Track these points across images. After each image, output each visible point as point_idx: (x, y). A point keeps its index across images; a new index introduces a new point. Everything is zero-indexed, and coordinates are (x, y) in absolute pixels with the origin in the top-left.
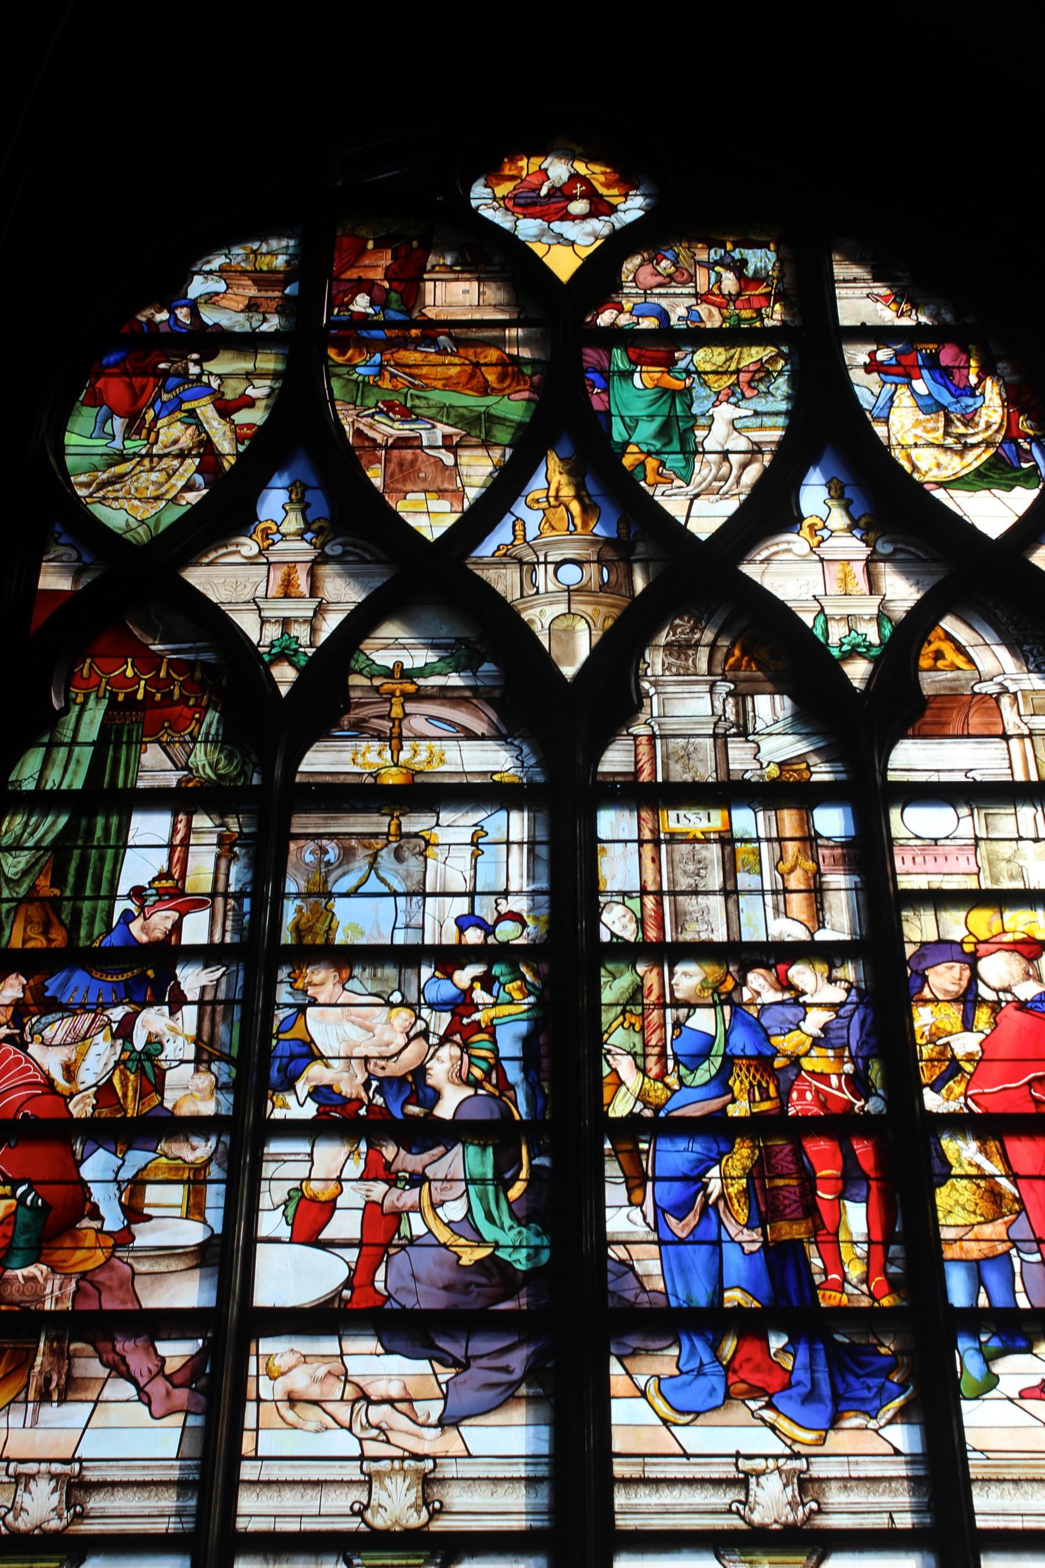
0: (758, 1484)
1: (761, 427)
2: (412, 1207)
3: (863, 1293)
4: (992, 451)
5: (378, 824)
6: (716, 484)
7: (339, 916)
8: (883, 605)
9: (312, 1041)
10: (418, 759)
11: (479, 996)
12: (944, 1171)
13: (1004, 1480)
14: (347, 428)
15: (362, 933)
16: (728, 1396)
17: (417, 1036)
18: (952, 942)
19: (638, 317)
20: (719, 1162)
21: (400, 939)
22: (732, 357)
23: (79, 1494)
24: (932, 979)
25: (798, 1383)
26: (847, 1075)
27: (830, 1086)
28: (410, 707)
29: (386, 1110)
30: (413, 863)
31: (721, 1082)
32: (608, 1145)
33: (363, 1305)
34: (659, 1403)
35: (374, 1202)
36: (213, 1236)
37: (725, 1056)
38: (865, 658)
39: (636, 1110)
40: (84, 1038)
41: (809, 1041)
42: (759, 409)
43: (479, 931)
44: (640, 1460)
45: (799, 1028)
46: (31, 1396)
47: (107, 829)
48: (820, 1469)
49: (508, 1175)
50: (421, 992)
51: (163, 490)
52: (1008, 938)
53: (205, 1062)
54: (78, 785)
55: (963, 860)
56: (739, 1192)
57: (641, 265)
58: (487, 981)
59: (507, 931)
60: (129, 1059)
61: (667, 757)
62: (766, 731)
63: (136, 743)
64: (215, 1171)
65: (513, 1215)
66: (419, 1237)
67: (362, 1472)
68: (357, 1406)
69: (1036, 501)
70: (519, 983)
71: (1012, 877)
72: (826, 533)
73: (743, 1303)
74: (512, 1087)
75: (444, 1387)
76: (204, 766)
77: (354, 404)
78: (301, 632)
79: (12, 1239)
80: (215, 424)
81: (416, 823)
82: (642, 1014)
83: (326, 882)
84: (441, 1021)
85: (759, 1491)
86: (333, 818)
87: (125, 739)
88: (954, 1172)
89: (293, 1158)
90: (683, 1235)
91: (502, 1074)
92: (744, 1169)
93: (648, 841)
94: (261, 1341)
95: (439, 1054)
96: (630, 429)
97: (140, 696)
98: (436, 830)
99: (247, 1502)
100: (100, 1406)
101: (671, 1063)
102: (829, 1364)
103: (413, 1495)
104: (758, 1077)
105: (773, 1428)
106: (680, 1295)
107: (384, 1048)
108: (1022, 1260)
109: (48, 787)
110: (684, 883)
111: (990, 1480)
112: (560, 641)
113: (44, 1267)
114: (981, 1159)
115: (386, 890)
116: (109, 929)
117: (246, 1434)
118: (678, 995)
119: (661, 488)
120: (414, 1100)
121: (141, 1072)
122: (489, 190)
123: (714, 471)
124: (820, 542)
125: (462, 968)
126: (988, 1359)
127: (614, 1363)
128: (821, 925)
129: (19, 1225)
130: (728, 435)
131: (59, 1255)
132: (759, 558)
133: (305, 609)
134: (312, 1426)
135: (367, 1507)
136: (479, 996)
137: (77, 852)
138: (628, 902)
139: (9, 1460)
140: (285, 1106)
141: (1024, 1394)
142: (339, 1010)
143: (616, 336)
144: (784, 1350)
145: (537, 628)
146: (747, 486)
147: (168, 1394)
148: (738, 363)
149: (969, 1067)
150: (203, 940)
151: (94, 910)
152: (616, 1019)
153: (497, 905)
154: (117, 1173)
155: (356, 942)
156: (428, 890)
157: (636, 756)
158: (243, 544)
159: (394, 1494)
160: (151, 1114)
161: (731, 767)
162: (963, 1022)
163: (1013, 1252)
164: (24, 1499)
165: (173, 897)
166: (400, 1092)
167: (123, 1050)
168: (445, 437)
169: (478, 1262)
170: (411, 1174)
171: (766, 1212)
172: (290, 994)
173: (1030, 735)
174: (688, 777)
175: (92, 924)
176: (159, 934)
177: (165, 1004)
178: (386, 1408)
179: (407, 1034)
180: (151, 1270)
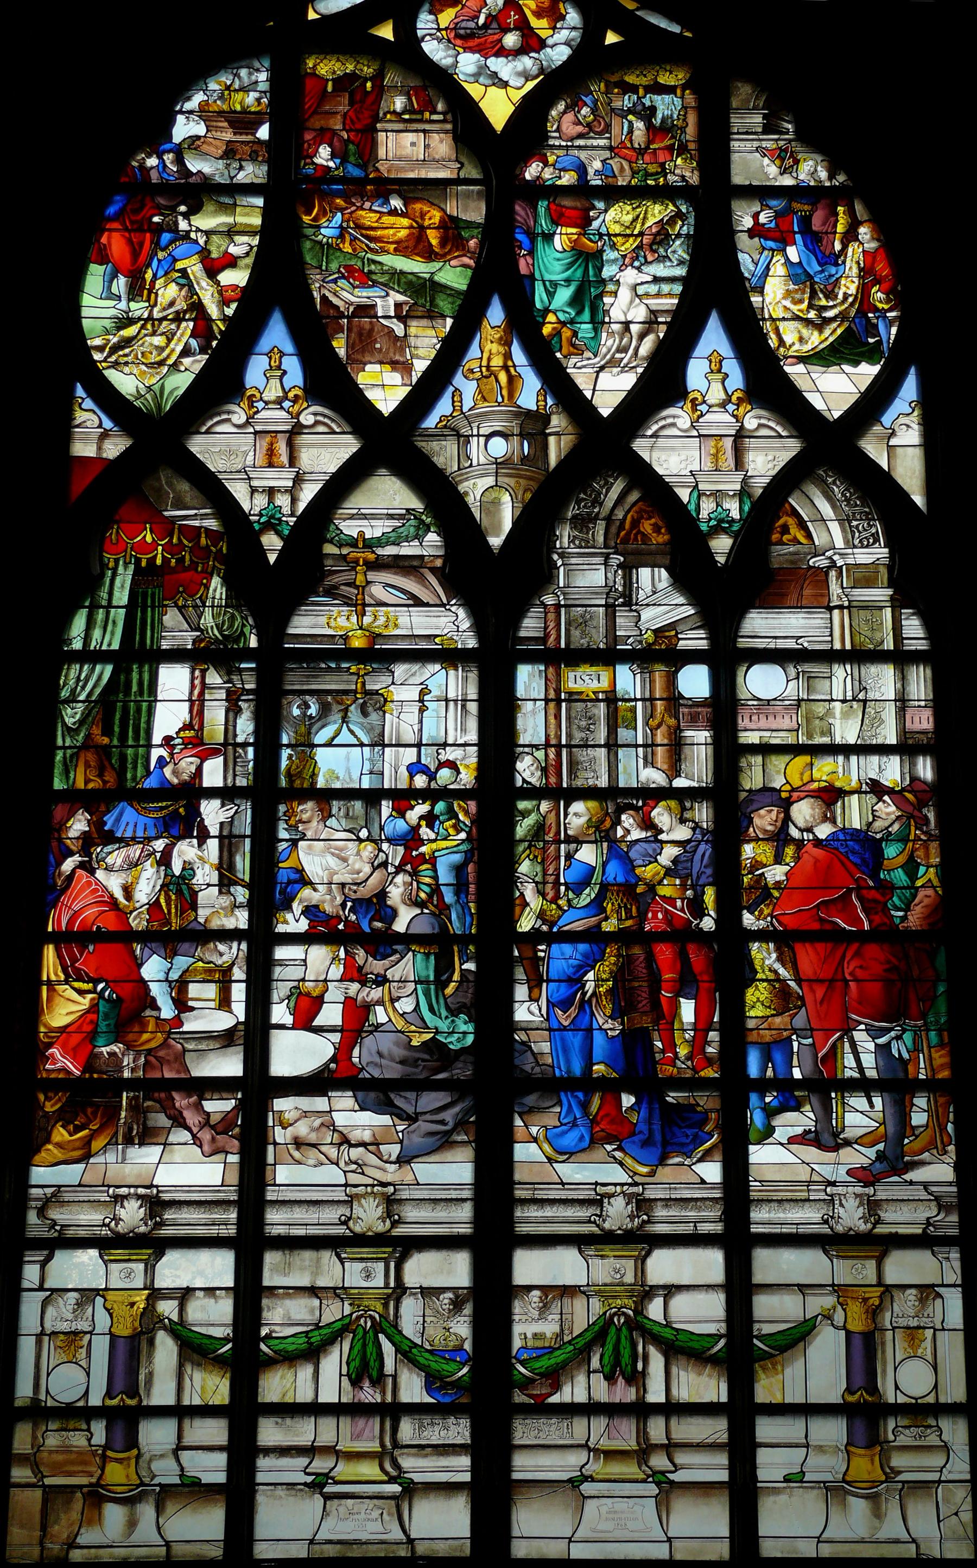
1: (658, 295)
4: (846, 324)
5: (348, 682)
6: (618, 356)
7: (319, 764)
8: (745, 481)
9: (303, 869)
11: (425, 832)
12: (751, 976)
14: (315, 294)
15: (338, 778)
16: (592, 1141)
17: (379, 866)
18: (774, 789)
19: (560, 170)
21: (365, 785)
22: (638, 216)
24: (757, 821)
25: (640, 1132)
26: (689, 899)
27: (675, 908)
28: (371, 576)
30: (374, 717)
31: (597, 905)
32: (516, 953)
33: (344, 1075)
34: (546, 1147)
36: (238, 1023)
37: (601, 884)
38: (727, 533)
40: (136, 865)
41: (662, 873)
42: (658, 275)
45: (656, 861)
46: (120, 1141)
47: (140, 683)
48: (651, 1194)
50: (382, 828)
51: (165, 354)
52: (815, 785)
54: (116, 646)
55: (787, 718)
57: (564, 112)
59: (444, 775)
60: (170, 883)
61: (568, 623)
64: (238, 973)
65: (448, 1008)
68: (342, 1148)
69: (877, 377)
71: (823, 734)
72: (704, 408)
74: (448, 907)
77: (320, 267)
78: (283, 501)
79: (97, 1025)
80: (204, 284)
83: (309, 733)
84: (396, 854)
86: (314, 676)
88: (759, 976)
90: (566, 1023)
91: (441, 897)
93: (552, 700)
96: (551, 295)
97: (159, 561)
98: (391, 688)
99: (273, 1216)
100: (168, 1148)
101: (563, 888)
105: (621, 1164)
109: (92, 648)
110: (578, 737)
112: (489, 513)
114: (777, 966)
115: (355, 742)
116: (148, 773)
118: (570, 832)
119: (573, 360)
121: (179, 893)
122: (432, 17)
123: (617, 341)
124: (699, 417)
125: (412, 808)
126: (770, 1113)
127: (516, 1116)
130: (632, 302)
131: (131, 1037)
132: (649, 433)
133: (284, 479)
134: (311, 1162)
135: (350, 1218)
136: (425, 832)
139: (109, 1186)
140: (286, 922)
141: (792, 1140)
143: (539, 190)
145: (470, 500)
146: (644, 358)
147: (213, 1139)
148: (643, 224)
149: (776, 894)
150: (219, 783)
151: (136, 755)
152: (524, 852)
154: (167, 974)
158: (234, 412)
161: (618, 633)
164: (122, 1213)
165: (195, 746)
166: (367, 913)
167: (166, 875)
168: (398, 306)
169: (424, 1043)
170: (377, 975)
173: (849, 607)
175: (135, 768)
176: (185, 777)
178: (361, 1149)
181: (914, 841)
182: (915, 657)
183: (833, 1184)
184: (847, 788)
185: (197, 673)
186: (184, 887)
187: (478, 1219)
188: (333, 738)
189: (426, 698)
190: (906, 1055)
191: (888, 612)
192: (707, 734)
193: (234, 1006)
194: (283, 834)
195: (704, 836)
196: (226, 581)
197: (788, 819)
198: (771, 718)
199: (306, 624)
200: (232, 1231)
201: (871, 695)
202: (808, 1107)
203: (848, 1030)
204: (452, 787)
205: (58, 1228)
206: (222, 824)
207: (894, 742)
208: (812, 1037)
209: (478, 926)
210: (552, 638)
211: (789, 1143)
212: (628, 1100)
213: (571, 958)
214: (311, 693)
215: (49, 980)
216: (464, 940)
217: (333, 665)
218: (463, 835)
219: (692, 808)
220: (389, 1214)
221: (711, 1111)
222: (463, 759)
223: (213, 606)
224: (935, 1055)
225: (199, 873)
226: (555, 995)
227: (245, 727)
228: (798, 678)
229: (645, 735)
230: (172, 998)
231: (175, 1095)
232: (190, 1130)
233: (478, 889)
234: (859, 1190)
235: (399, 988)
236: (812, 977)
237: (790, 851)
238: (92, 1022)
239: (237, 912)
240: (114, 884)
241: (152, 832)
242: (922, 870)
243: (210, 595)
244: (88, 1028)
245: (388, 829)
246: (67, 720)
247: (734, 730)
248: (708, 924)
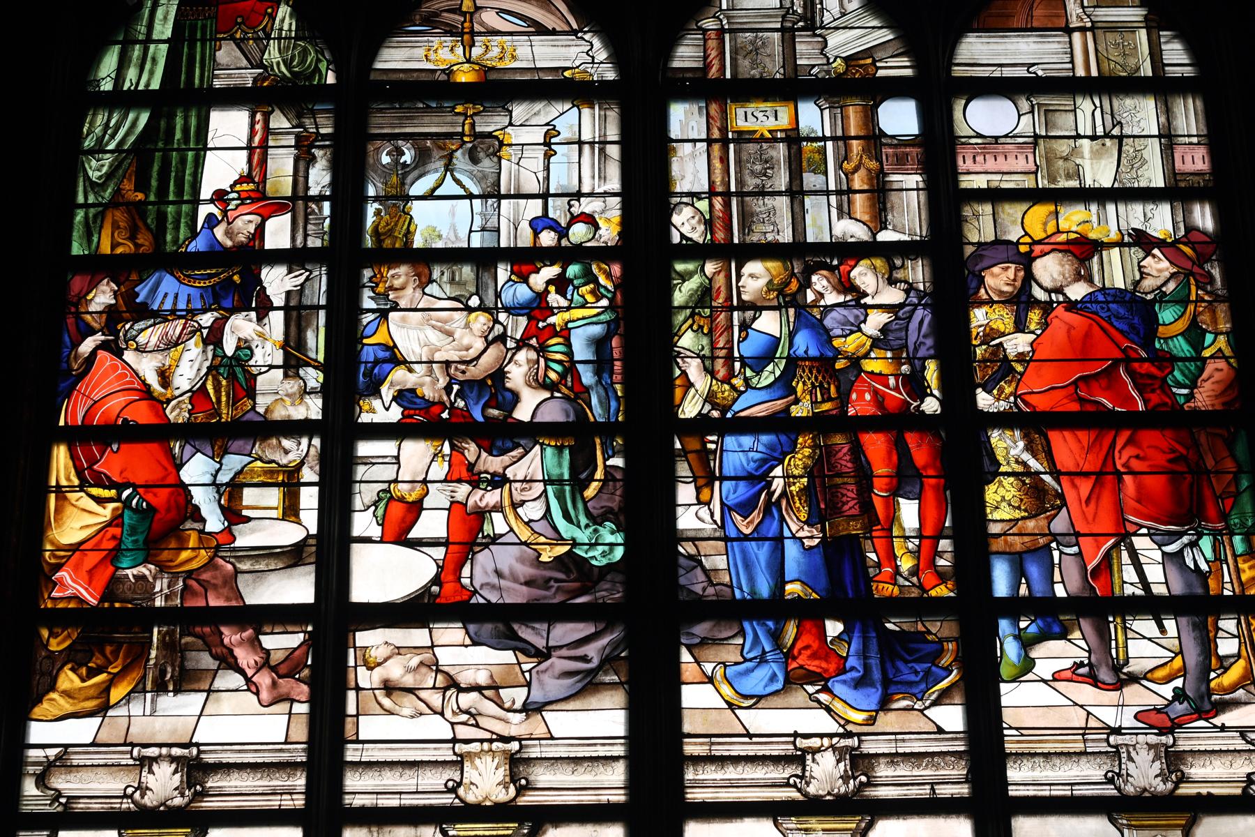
0: (814, 760)
2: (494, 507)
3: (914, 585)
5: (453, 124)
7: (416, 220)
9: (395, 346)
10: (488, 56)
11: (554, 299)
12: (992, 469)
13: (1035, 754)
15: (440, 236)
16: (789, 681)
17: (495, 340)
18: (1009, 242)
20: (782, 462)
21: (476, 242)
23: (199, 775)
24: (989, 281)
25: (853, 669)
26: (904, 376)
27: (888, 387)
30: (487, 164)
31: (784, 384)
32: (678, 445)
34: (726, 690)
35: (458, 502)
36: (309, 536)
37: (789, 358)
39: (705, 411)
40: (176, 344)
41: (869, 344)
43: (552, 234)
44: (708, 740)
45: (860, 330)
46: (149, 687)
47: (186, 130)
48: (870, 747)
49: (583, 476)
50: (498, 295)
52: (1063, 238)
53: (293, 367)
55: (1022, 159)
56: (801, 490)
58: (561, 284)
59: (579, 232)
60: (220, 365)
61: (735, 52)
62: (832, 25)
63: (211, 40)
64: (309, 475)
65: (588, 514)
66: (502, 536)
67: (455, 754)
68: (448, 693)
70: (592, 286)
71: (1069, 177)
73: (802, 594)
74: (587, 390)
75: (527, 675)
76: (278, 64)
81: (490, 124)
82: (710, 316)
83: (403, 184)
85: (814, 766)
87: (199, 35)
88: (1002, 469)
89: (380, 460)
90: (747, 531)
91: (576, 377)
92: (805, 468)
93: (716, 141)
94: (358, 634)
95: (516, 357)
98: (509, 130)
99: (353, 781)
100: (213, 696)
101: (737, 365)
102: (881, 650)
103: (502, 773)
104: (820, 378)
105: (829, 710)
106: (745, 589)
107: (465, 353)
108: (1061, 553)
109: (125, 88)
110: (751, 183)
111: (1023, 754)
113: (152, 567)
114: (1026, 457)
115: (462, 192)
117: (349, 720)
118: (745, 297)
120: (493, 403)
121: (232, 377)
125: (537, 271)
126: (1027, 643)
127: (684, 651)
128: (884, 226)
129: (126, 527)
131: (165, 555)
135: (459, 784)
136: (554, 299)
138: (699, 204)
139: (133, 745)
140: (372, 411)
141: (1057, 677)
142: (419, 314)
144: (839, 637)
147: (274, 684)
149: (1019, 368)
151: (179, 214)
152: (685, 322)
153: (571, 206)
154: (215, 476)
155: (434, 246)
156: (503, 191)
157: (705, 51)
159: (483, 773)
160: (245, 418)
161: (799, 62)
162: (1015, 322)
164: (149, 780)
165: (254, 201)
166: (479, 397)
167: (215, 356)
169: (556, 558)
170: (494, 475)
171: (826, 509)
172: (372, 298)
173: (1092, 29)
174: (755, 73)
175: (177, 228)
176: (242, 238)
177: (253, 309)
178: (474, 695)
179: (486, 338)
180: (252, 568)
181: (1196, 302)
182: (1179, 87)
183: (1117, 731)
184: (1105, 240)
185: (259, 117)
186: (238, 370)
187: (633, 784)
188: (434, 189)
189: (553, 140)
190: (1204, 567)
191: (1143, 35)
192: (919, 178)
193: (302, 514)
194: (368, 303)
195: (920, 299)
196: (296, 13)
197: (1029, 277)
198: (1001, 159)
199: (398, 58)
200: (299, 802)
201: (1127, 131)
202: (1077, 634)
203: (1124, 537)
204: (589, 244)
205: (63, 800)
206: (288, 293)
207: (1161, 184)
208: (1077, 544)
209: (626, 413)
210: (714, 69)
211: (1055, 680)
213: (751, 450)
214: (406, 137)
215: (58, 486)
216: (607, 430)
217: (434, 105)
218: (604, 302)
219: (903, 266)
220: (514, 778)
221: (948, 640)
222: (603, 212)
223: (279, 38)
225: (258, 353)
226: (732, 496)
227: (319, 178)
228: (1032, 112)
229: (838, 180)
230: (221, 506)
231: (226, 631)
232: (242, 672)
233: (625, 367)
234: (1153, 739)
235: (523, 490)
236: (1073, 469)
237: (1034, 316)
238: (114, 537)
239: (307, 399)
240: (147, 367)
241: (198, 304)
242: (1209, 338)
243: (277, 25)
244: (111, 545)
245: (507, 297)
246: (90, 173)
247: (954, 173)
248: (931, 406)
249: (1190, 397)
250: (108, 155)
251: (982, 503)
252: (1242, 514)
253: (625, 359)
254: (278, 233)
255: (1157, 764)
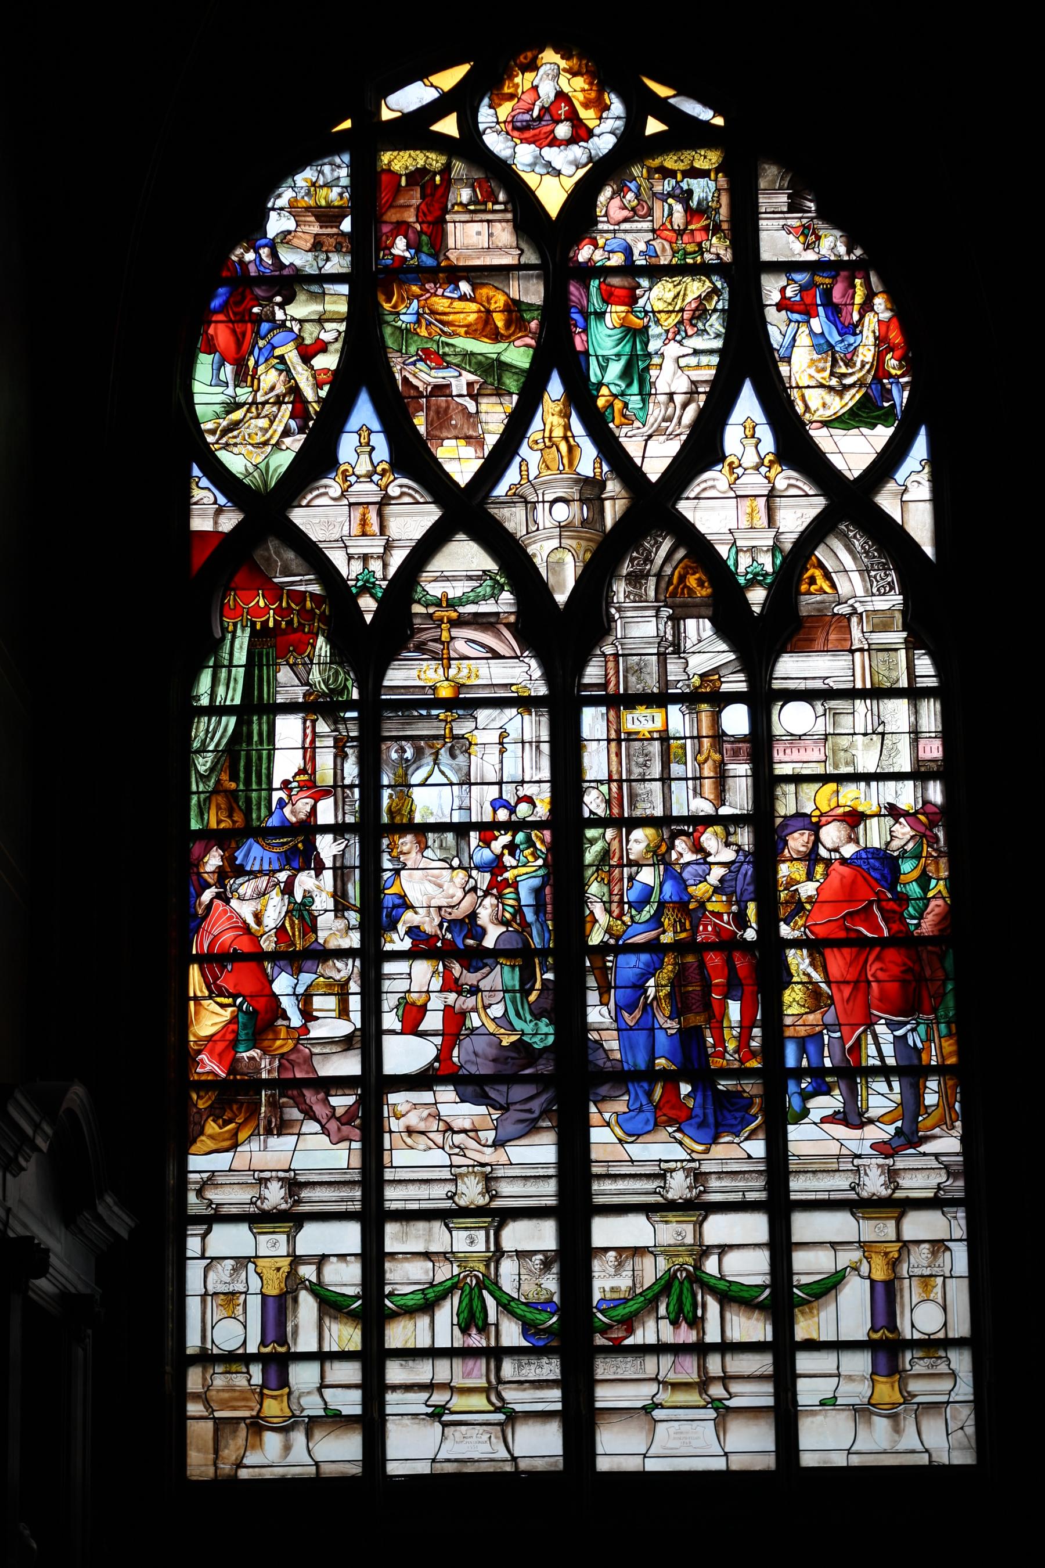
5: (438, 728)
7: (416, 802)
9: (405, 895)
11: (508, 860)
12: (788, 979)
13: (808, 1172)
15: (432, 813)
17: (470, 890)
18: (805, 815)
21: (456, 819)
24: (791, 843)
25: (696, 1116)
28: (455, 632)
29: (453, 942)
30: (461, 759)
31: (656, 920)
32: (588, 964)
33: (446, 1072)
36: (356, 1029)
39: (605, 940)
40: (264, 894)
41: (711, 891)
45: (706, 880)
47: (260, 734)
49: (528, 986)
50: (471, 857)
52: (841, 811)
59: (523, 809)
60: (293, 910)
61: (626, 670)
64: (354, 987)
65: (532, 1013)
66: (477, 1028)
74: (529, 925)
83: (406, 774)
84: (484, 880)
88: (795, 979)
90: (632, 1024)
93: (613, 740)
95: (484, 903)
101: (626, 907)
102: (714, 1104)
110: (636, 772)
111: (800, 1172)
114: (810, 970)
115: (446, 781)
118: (632, 857)
121: (301, 918)
125: (496, 838)
126: (806, 1096)
136: (508, 860)
137: (243, 753)
140: (392, 941)
141: (824, 1120)
144: (688, 1095)
149: (808, 907)
150: (332, 821)
151: (260, 798)
153: (517, 790)
154: (295, 989)
156: (473, 781)
157: (606, 670)
161: (669, 678)
163: (825, 1031)
165: (309, 788)
166: (461, 931)
167: (289, 903)
169: (512, 1043)
170: (471, 986)
175: (259, 809)
176: (302, 816)
183: (859, 1156)
184: (868, 812)
185: (308, 723)
186: (305, 913)
188: (427, 779)
189: (505, 740)
190: (920, 1045)
192: (747, 766)
193: (351, 1014)
194: (387, 864)
195: (746, 857)
197: (817, 840)
198: (802, 751)
203: (870, 1024)
206: (335, 856)
208: (840, 1031)
209: (555, 942)
212: (685, 1089)
216: (543, 953)
218: (540, 862)
221: (756, 1096)
222: (539, 794)
224: (945, 1044)
225: (317, 900)
227: (351, 771)
229: (694, 770)
230: (299, 1009)
234: (881, 1161)
236: (840, 979)
239: (351, 933)
240: (246, 911)
241: (276, 866)
245: (477, 858)
246: (199, 767)
247: (771, 762)
248: (750, 935)
249: (918, 926)
250: (210, 754)
251: (780, 1003)
252: (947, 1009)
253: (554, 904)
254: (326, 813)
255: (883, 1177)
